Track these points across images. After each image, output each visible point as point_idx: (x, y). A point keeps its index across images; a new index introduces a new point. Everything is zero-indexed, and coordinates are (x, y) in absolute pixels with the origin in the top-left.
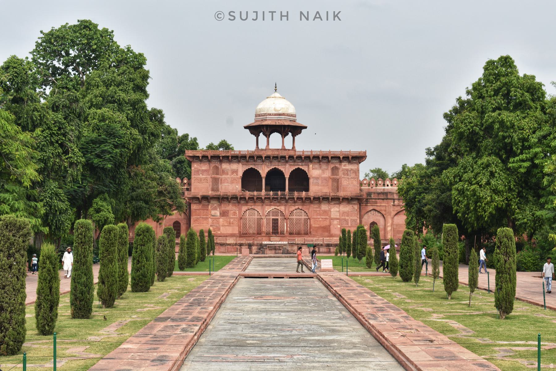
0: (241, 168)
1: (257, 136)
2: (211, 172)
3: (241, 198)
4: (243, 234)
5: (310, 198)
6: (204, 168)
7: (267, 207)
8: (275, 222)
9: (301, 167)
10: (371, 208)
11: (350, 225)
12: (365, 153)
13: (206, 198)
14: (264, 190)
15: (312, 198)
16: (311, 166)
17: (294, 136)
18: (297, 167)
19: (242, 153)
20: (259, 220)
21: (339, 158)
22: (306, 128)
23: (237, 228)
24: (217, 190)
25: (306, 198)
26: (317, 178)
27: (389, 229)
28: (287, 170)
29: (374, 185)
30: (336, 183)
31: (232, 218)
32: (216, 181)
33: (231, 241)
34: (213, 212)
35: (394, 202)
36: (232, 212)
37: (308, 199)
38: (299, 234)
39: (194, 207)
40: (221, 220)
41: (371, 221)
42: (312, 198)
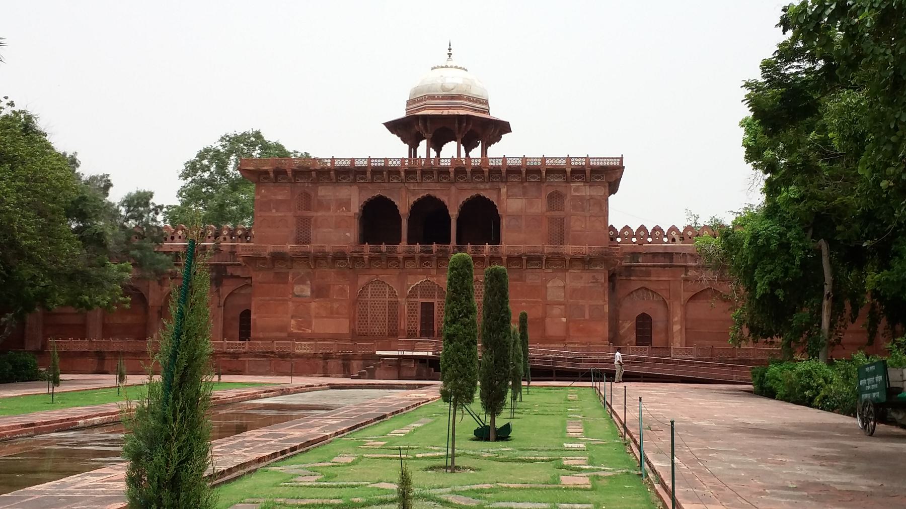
0: (355, 198)
3: (354, 260)
4: (360, 335)
6: (280, 197)
7: (410, 278)
9: (483, 194)
11: (587, 317)
13: (278, 257)
16: (504, 190)
18: (474, 193)
19: (357, 164)
26: (516, 217)
27: (676, 328)
28: (454, 201)
34: (297, 289)
35: (687, 271)
36: (337, 287)
39: (258, 277)
40: (313, 305)
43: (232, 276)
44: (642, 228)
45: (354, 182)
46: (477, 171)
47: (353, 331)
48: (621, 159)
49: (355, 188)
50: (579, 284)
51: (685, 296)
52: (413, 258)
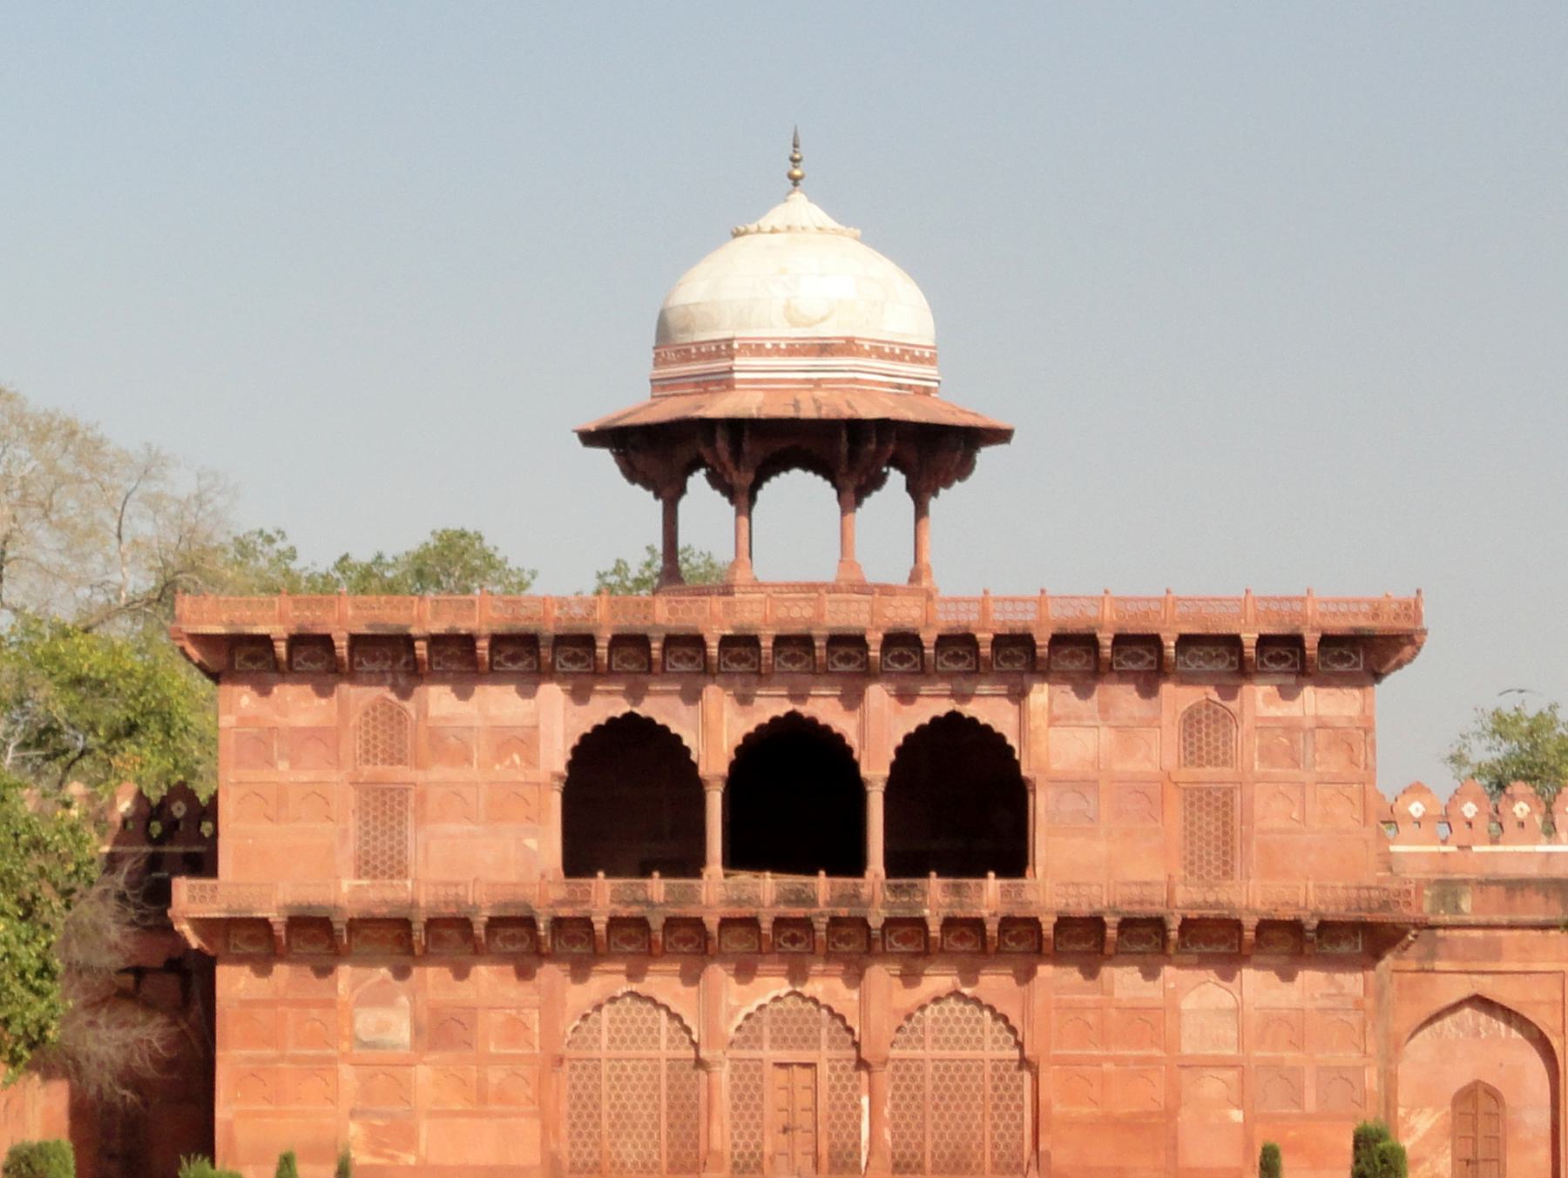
1: (670, 492)
2: (352, 744)
10: (1462, 988)
12: (1412, 609)
17: (921, 492)
21: (1234, 642)
22: (1000, 436)
23: (529, 1130)
24: (396, 868)
25: (1007, 922)
26: (1081, 784)
28: (876, 728)
29: (1482, 825)
30: (1217, 819)
31: (499, 1059)
32: (386, 806)
34: (366, 1021)
36: (497, 1017)
40: (423, 1073)
41: (1462, 1076)
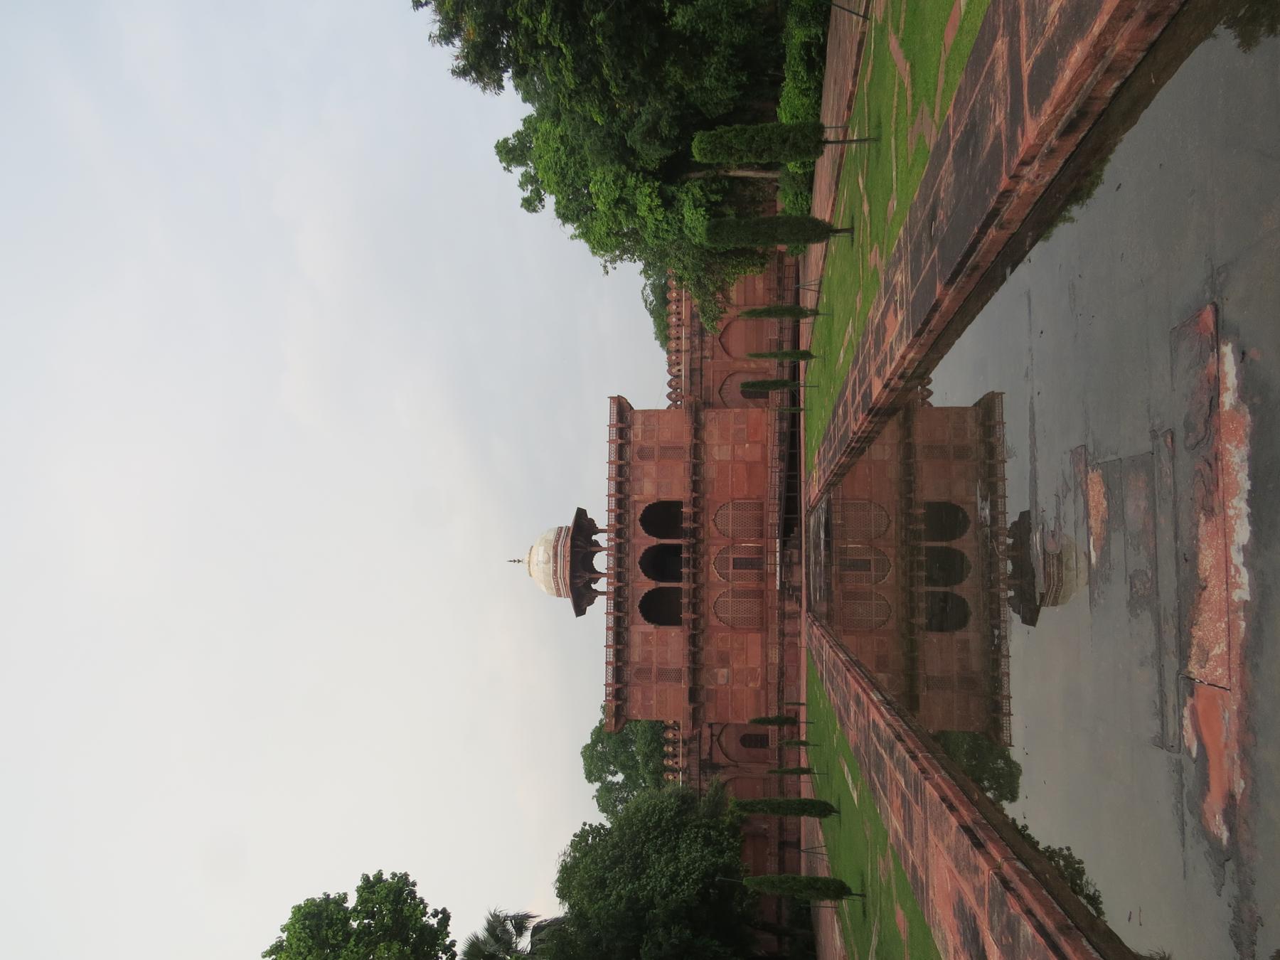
0: (641, 628)
3: (695, 628)
5: (695, 499)
6: (640, 697)
8: (738, 564)
9: (639, 516)
13: (693, 694)
14: (680, 585)
15: (694, 495)
16: (636, 497)
18: (638, 523)
19: (611, 625)
20: (736, 594)
25: (694, 506)
27: (753, 365)
28: (643, 541)
30: (667, 451)
32: (663, 674)
33: (774, 656)
34: (721, 681)
37: (695, 502)
38: (761, 520)
39: (711, 717)
40: (735, 666)
42: (694, 495)
43: (710, 754)
44: (669, 396)
45: (627, 629)
46: (619, 533)
47: (759, 630)
48: (611, 398)
49: (633, 628)
50: (716, 433)
51: (726, 358)
52: (695, 575)
